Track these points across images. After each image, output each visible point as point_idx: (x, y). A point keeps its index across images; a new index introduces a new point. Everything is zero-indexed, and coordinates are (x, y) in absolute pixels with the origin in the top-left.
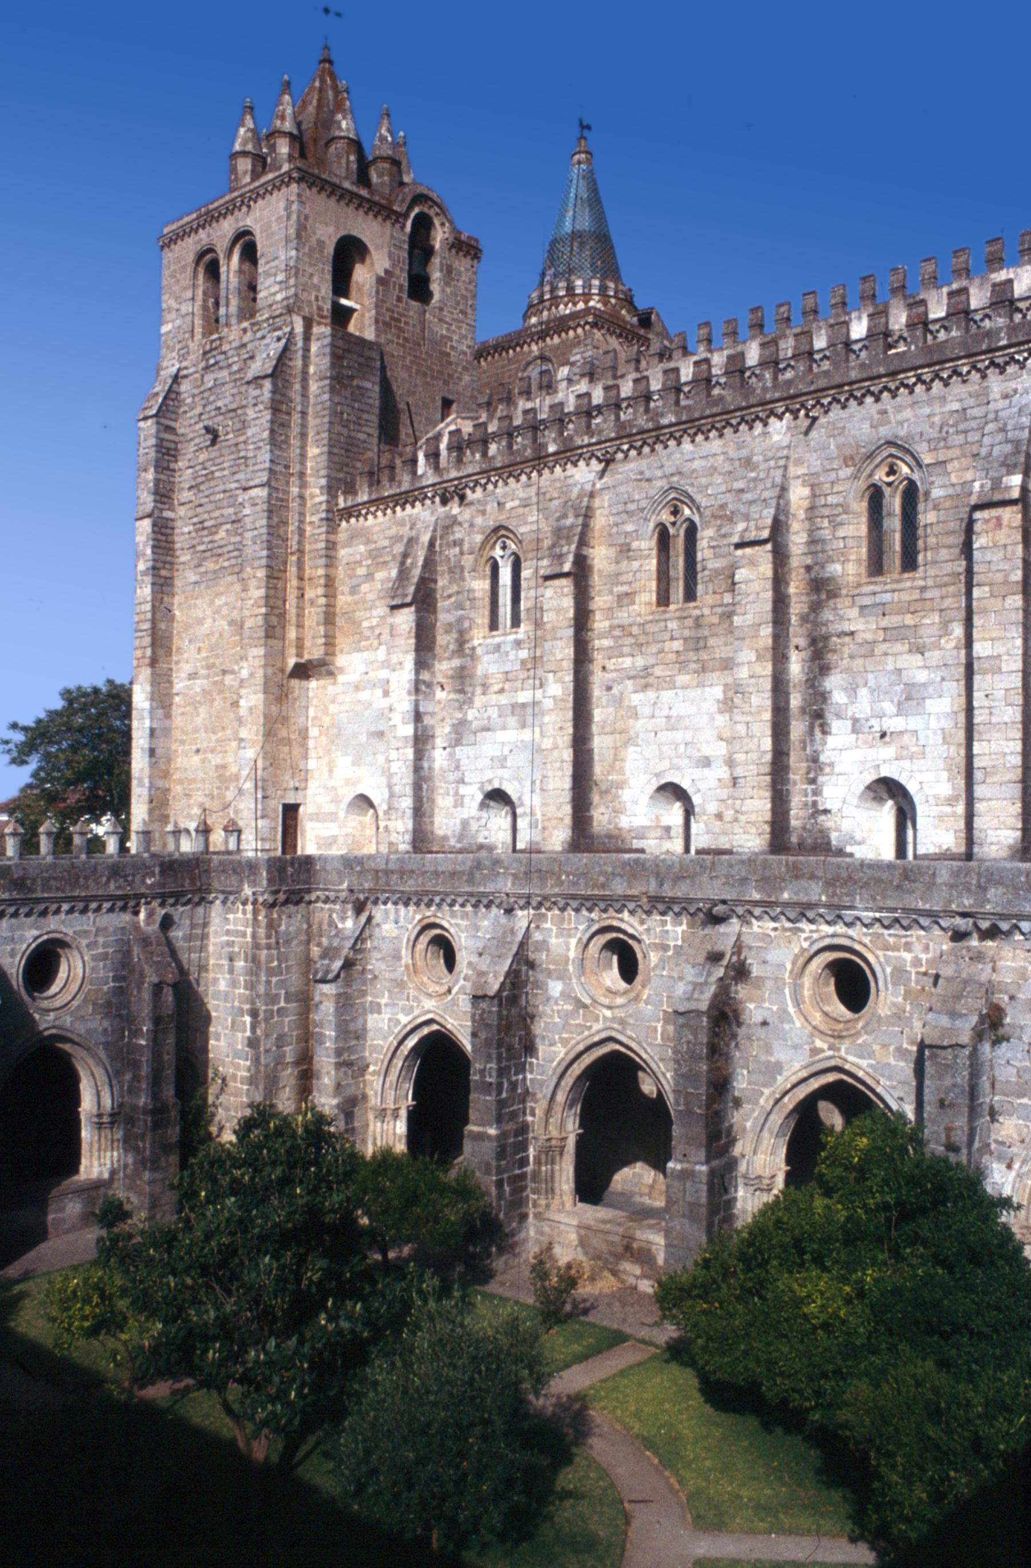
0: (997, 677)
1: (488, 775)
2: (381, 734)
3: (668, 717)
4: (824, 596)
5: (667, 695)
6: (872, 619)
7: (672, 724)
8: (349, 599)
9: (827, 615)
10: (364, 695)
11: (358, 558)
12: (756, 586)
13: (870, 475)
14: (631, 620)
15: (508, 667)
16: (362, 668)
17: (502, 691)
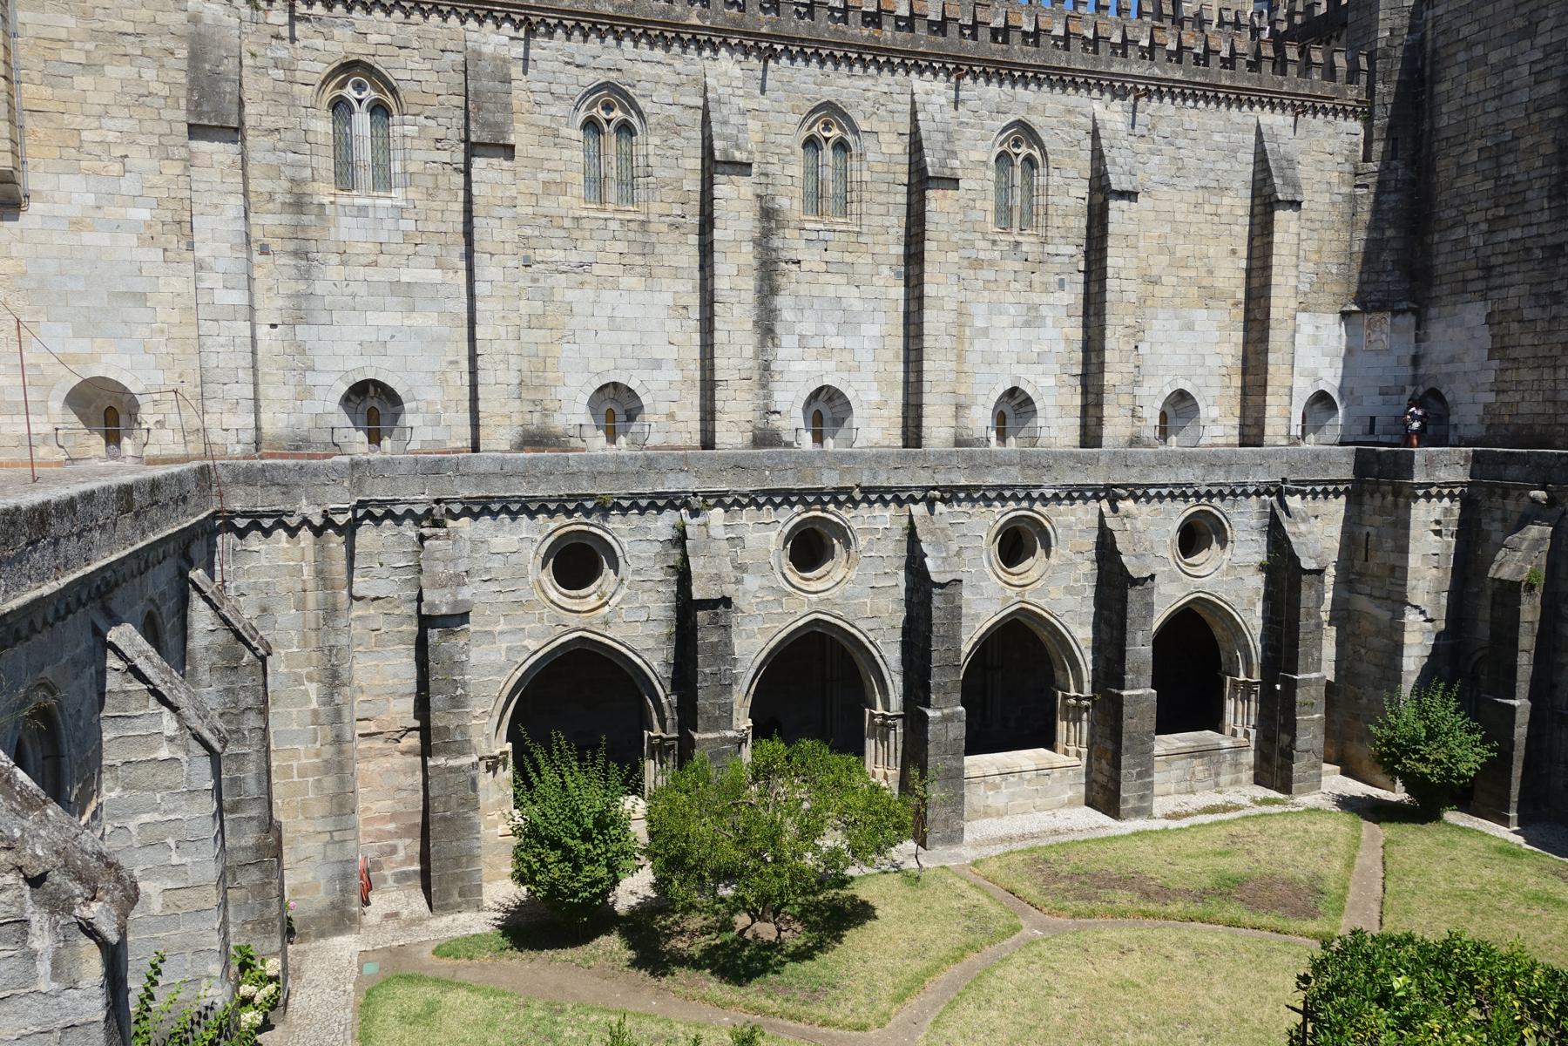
0: (941, 313)
1: (352, 364)
2: (140, 298)
3: (611, 318)
4: (773, 225)
5: (609, 296)
6: (814, 251)
7: (614, 324)
8: (47, 92)
9: (776, 242)
10: (100, 239)
11: (63, 35)
12: (736, 205)
13: (810, 128)
14: (562, 212)
15: (383, 237)
16: (90, 199)
17: (375, 264)
